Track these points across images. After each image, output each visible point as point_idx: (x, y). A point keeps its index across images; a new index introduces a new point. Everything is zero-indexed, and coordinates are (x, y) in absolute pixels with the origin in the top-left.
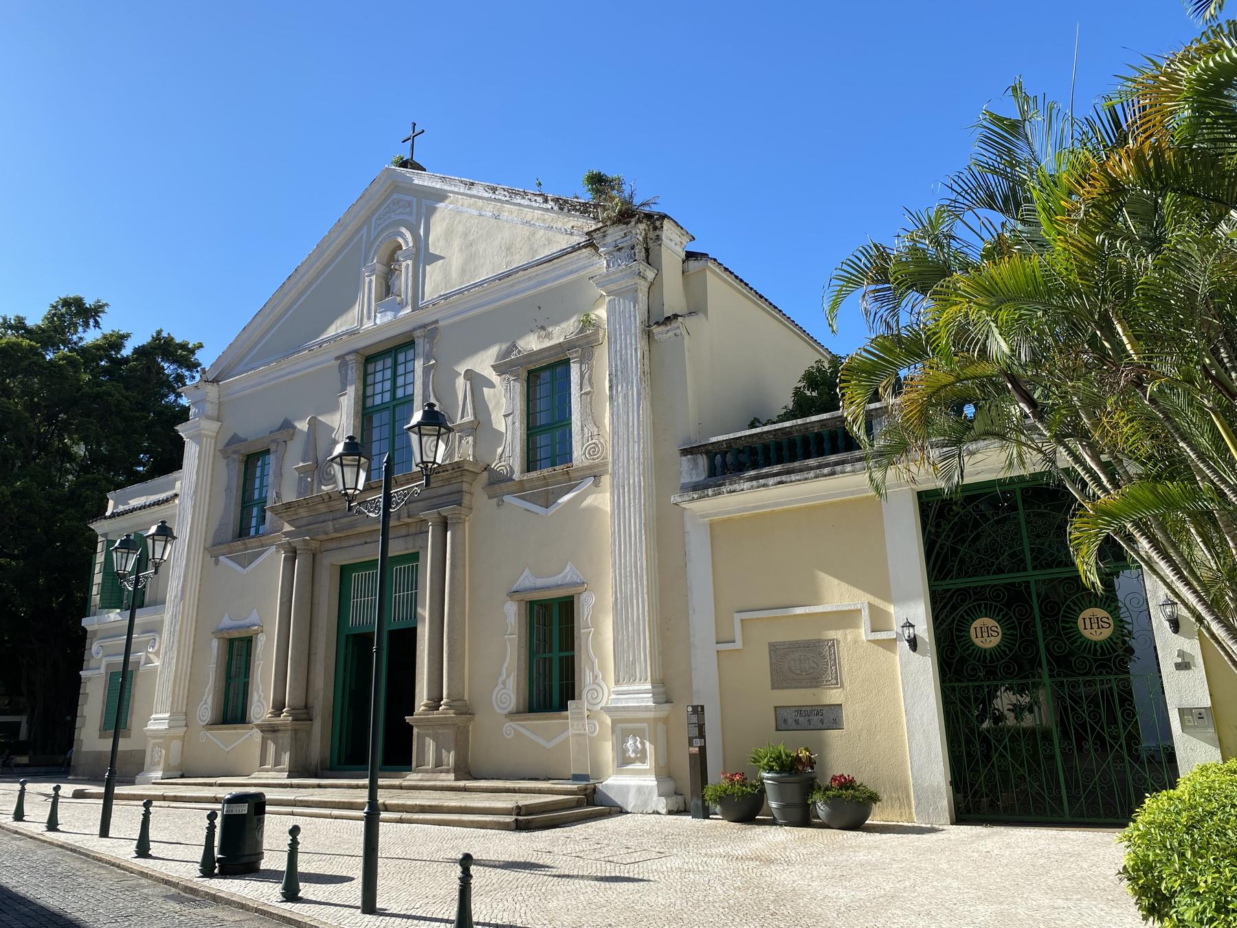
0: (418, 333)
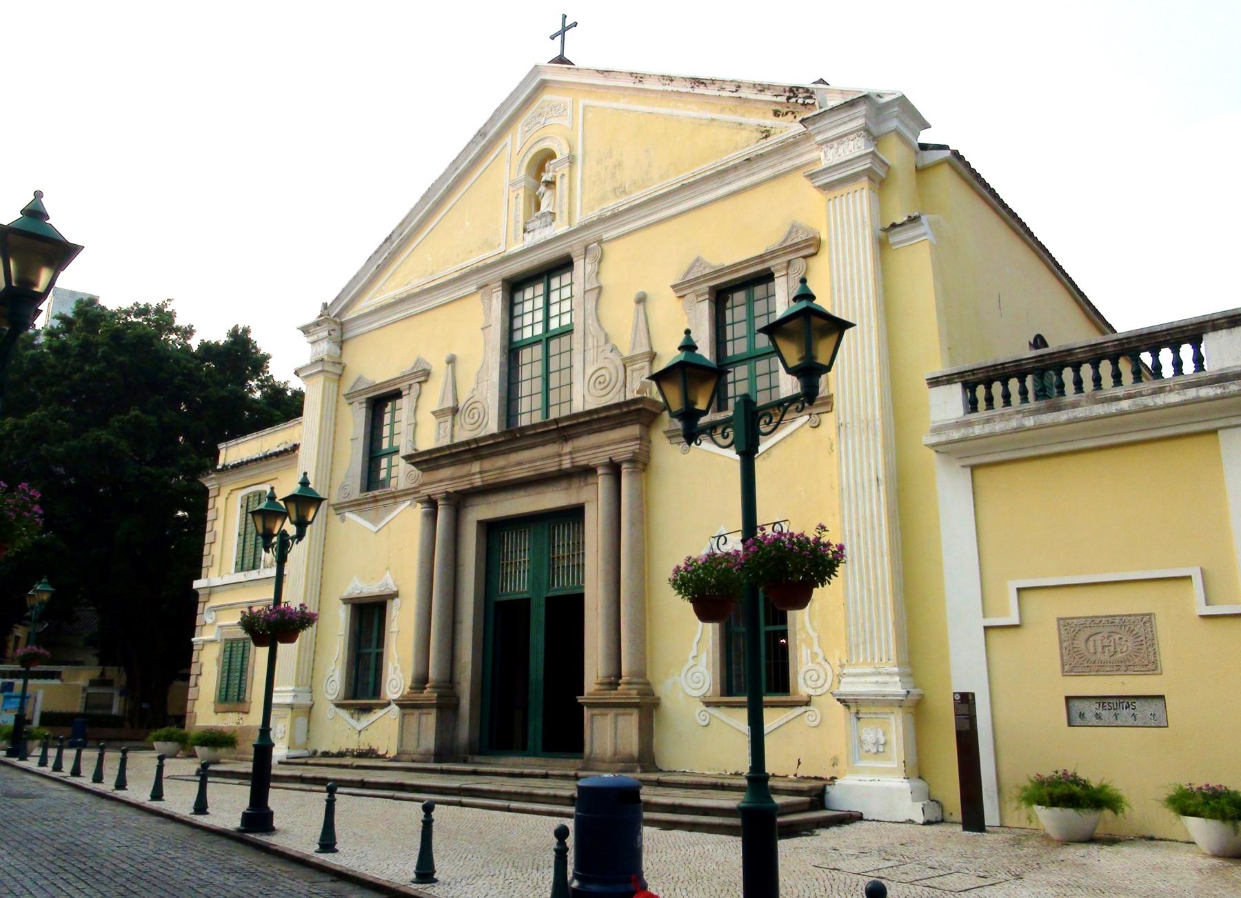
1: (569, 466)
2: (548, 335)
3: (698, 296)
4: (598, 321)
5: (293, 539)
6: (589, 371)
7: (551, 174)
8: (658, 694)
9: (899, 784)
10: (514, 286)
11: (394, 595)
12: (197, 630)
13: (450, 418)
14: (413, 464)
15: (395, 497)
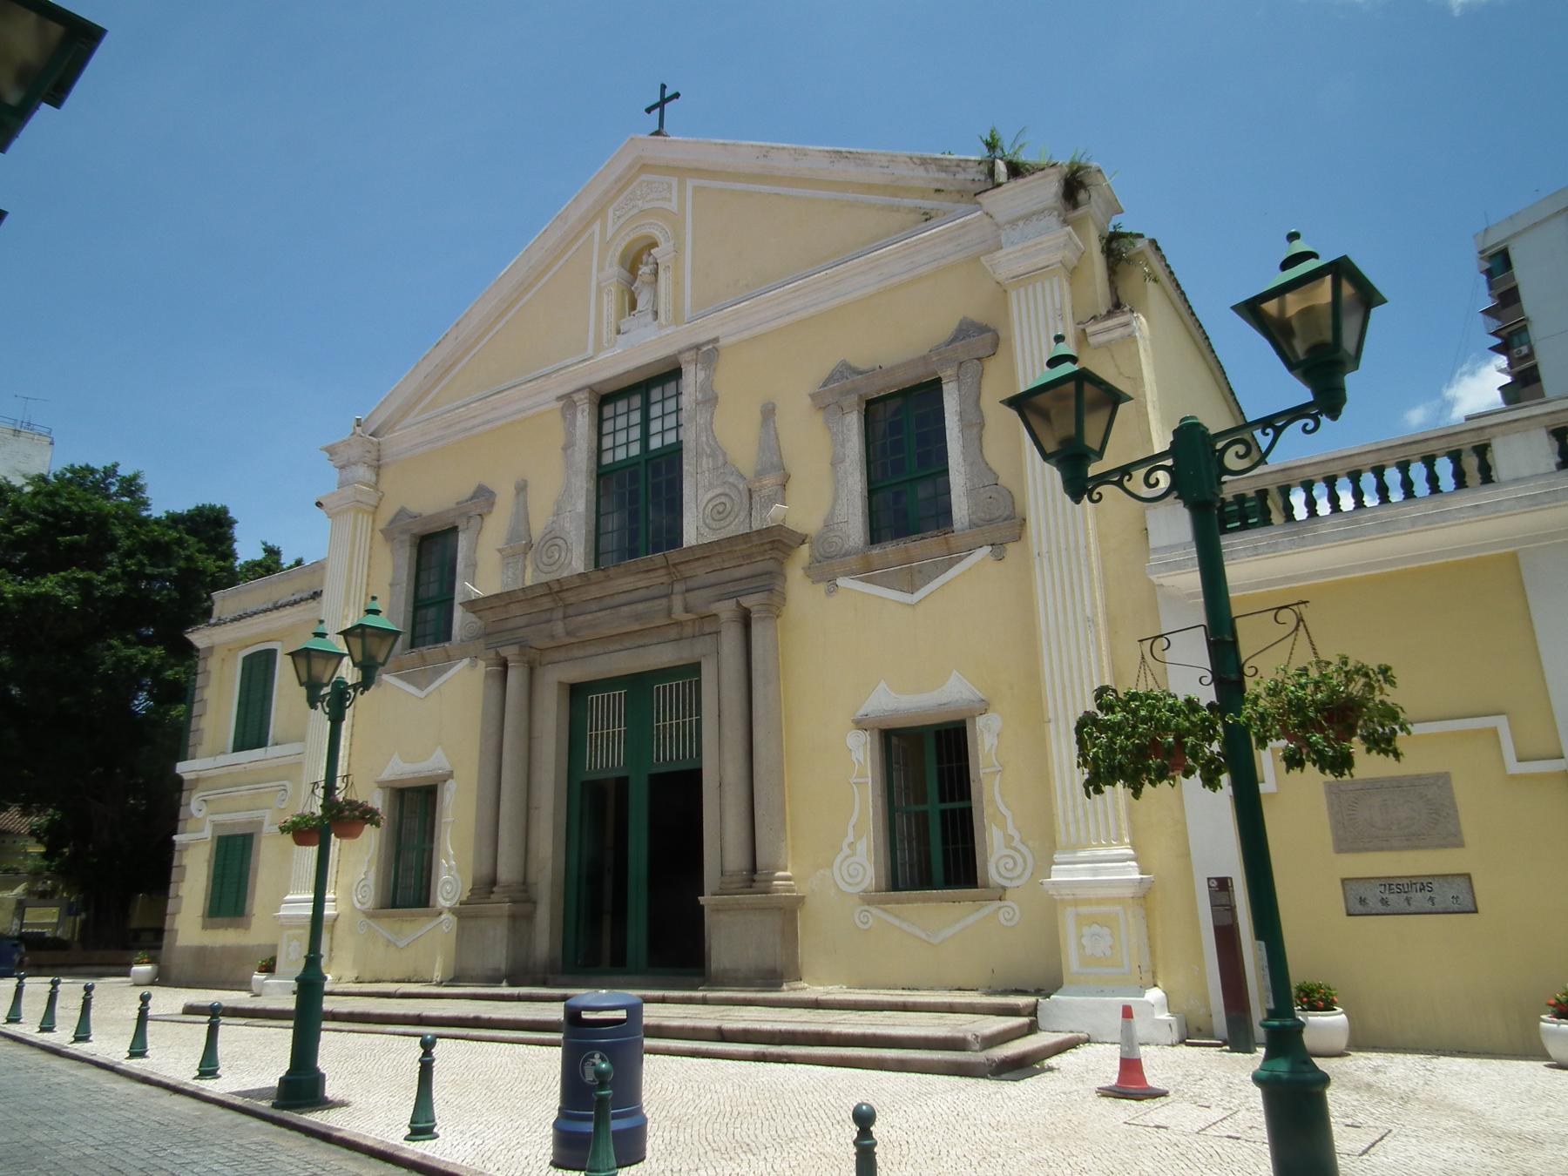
0: (688, 356)
10: (605, 399)
11: (450, 775)
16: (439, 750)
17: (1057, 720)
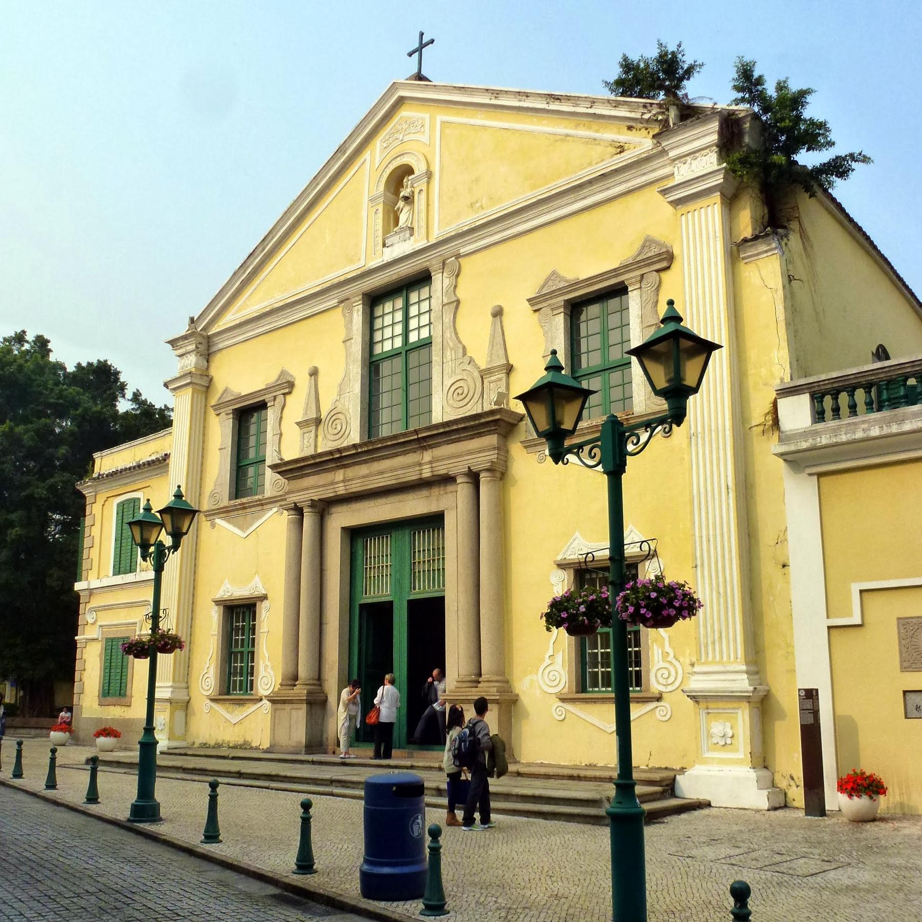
1: (429, 475)
2: (408, 348)
3: (553, 310)
4: (456, 334)
5: (169, 548)
6: (448, 383)
7: (409, 190)
8: (517, 692)
9: (749, 774)
10: (374, 299)
11: (264, 598)
12: (80, 628)
13: (314, 428)
14: (279, 473)
15: (262, 505)
16: (257, 578)
17: (702, 565)
